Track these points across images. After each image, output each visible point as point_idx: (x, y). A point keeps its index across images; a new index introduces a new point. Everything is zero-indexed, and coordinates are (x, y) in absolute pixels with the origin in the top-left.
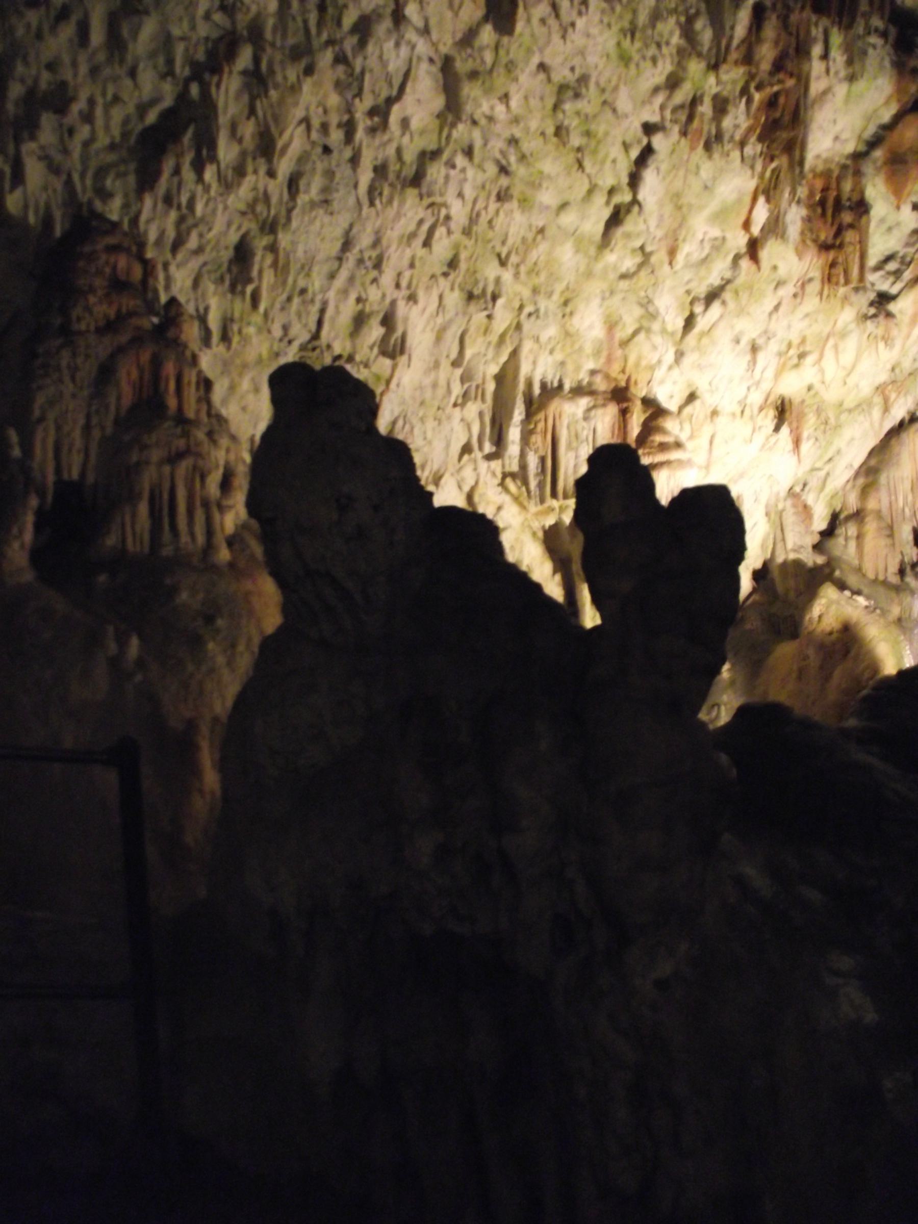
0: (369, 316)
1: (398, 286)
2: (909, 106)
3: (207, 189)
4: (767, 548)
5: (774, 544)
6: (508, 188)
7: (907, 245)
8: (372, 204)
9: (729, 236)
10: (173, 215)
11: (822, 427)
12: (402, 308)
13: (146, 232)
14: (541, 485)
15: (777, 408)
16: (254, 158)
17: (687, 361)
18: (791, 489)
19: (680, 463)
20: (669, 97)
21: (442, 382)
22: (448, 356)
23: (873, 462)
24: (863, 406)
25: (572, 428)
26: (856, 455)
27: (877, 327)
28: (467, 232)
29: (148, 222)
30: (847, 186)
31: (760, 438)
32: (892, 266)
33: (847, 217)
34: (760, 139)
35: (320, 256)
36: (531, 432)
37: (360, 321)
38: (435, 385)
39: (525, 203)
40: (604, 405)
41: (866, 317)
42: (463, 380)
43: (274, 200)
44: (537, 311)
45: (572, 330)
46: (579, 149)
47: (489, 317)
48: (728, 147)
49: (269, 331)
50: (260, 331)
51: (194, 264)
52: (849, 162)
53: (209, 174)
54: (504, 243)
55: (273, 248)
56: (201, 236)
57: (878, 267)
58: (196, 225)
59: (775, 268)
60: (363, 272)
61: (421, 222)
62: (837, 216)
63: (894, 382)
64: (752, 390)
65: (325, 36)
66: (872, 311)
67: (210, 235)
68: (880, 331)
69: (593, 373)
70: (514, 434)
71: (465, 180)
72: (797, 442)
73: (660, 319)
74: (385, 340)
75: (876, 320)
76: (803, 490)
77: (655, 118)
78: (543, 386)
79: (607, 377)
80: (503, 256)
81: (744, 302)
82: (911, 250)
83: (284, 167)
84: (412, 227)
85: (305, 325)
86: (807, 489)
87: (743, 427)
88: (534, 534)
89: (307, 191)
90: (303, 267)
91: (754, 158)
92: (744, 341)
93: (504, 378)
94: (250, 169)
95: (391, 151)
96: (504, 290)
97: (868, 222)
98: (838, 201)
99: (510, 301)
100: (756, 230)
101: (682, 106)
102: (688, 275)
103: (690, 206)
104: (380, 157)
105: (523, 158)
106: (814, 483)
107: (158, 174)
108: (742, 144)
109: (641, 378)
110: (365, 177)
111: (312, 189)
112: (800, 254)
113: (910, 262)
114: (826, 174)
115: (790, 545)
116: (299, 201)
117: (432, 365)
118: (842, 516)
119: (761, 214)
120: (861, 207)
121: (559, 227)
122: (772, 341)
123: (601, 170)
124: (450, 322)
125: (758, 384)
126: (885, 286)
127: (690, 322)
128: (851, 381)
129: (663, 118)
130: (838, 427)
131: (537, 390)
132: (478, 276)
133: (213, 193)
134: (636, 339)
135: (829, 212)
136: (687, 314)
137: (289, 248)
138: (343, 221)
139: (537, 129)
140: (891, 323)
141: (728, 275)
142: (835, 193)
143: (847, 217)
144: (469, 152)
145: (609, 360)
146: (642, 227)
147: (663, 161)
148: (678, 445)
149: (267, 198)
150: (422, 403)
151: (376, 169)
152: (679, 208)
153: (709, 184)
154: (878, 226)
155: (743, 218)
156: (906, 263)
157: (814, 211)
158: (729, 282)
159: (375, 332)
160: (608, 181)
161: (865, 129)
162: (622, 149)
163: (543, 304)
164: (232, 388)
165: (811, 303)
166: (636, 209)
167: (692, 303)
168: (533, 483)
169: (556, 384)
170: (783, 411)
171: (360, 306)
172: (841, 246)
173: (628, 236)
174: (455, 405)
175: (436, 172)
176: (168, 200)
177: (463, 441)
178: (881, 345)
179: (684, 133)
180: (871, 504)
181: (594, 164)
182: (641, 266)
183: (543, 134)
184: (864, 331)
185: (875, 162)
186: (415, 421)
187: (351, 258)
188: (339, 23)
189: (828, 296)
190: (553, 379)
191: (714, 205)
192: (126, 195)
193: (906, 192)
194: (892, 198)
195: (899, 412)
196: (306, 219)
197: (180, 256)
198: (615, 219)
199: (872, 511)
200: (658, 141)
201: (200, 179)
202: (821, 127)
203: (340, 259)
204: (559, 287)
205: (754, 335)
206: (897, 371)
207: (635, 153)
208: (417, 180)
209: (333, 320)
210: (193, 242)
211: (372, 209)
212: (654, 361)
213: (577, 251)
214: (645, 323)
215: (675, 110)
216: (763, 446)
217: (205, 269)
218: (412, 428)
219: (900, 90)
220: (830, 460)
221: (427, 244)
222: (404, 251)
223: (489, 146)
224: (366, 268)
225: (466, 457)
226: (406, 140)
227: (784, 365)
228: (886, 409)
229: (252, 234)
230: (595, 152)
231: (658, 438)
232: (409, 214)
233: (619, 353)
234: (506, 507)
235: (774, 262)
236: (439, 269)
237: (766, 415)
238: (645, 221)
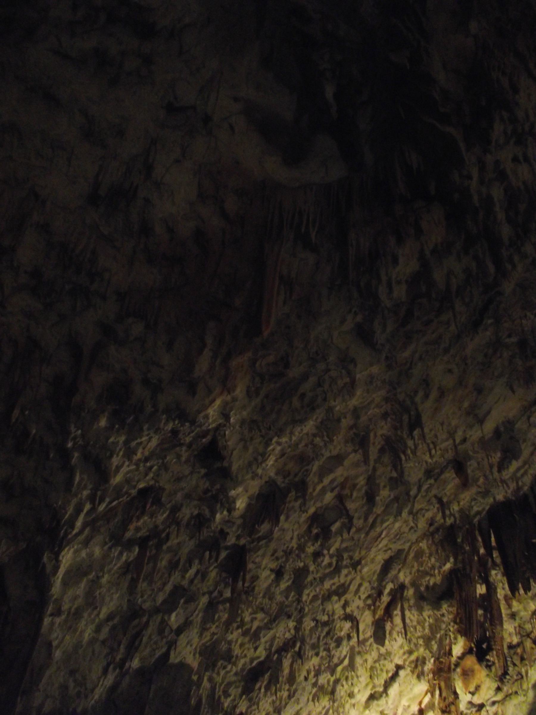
2: (468, 651)
7: (467, 709)
16: (285, 684)
20: (408, 657)
65: (324, 642)
82: (469, 712)
101: (413, 661)
166: (384, 695)
188: (332, 639)
191: (411, 696)
198: (372, 697)
207: (390, 674)
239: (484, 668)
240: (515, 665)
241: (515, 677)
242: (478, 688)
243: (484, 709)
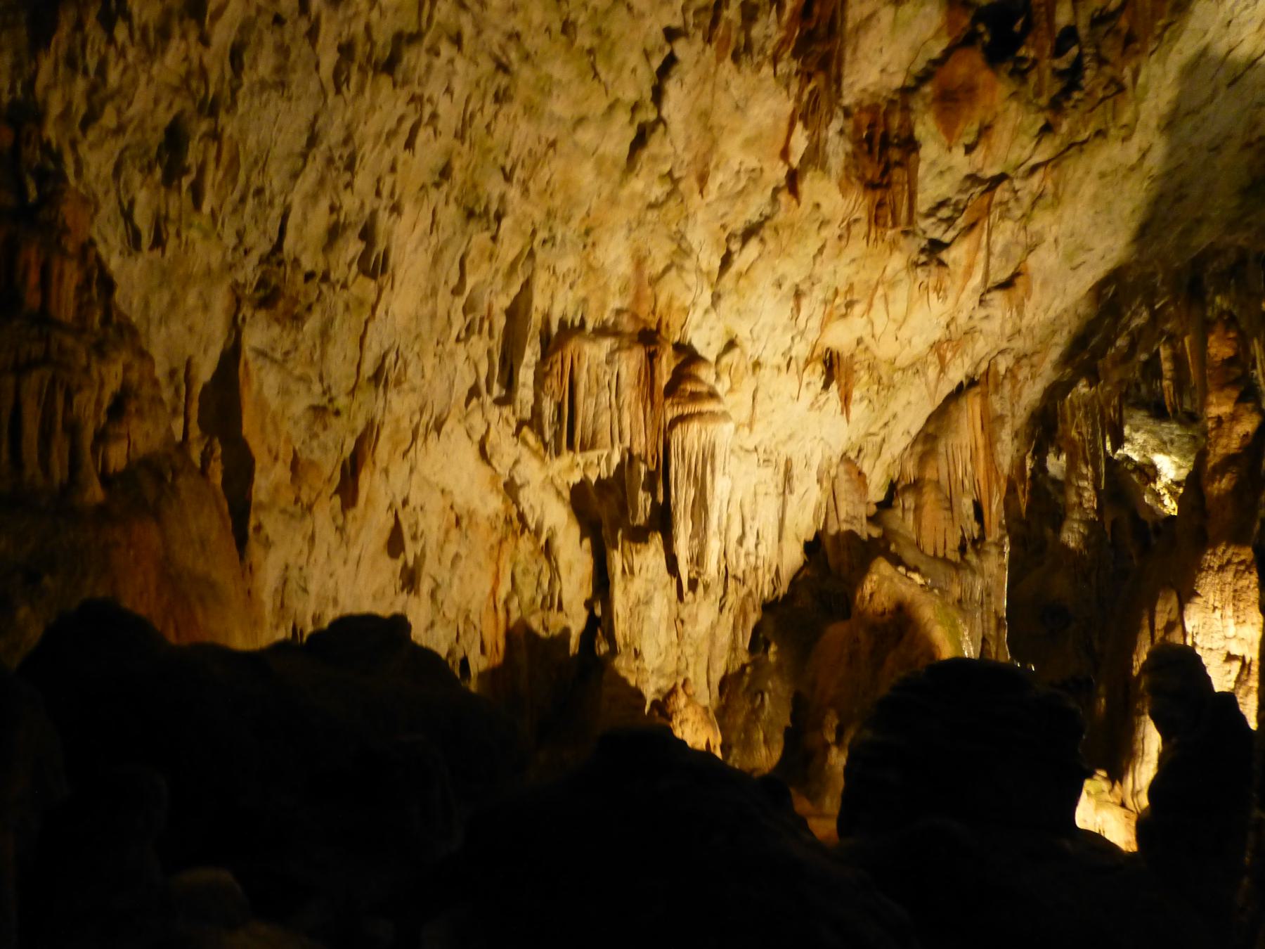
0: (345, 227)
1: (378, 194)
3: (122, 54)
4: (819, 518)
5: (827, 514)
6: (507, 89)
7: (960, 191)
8: (338, 91)
9: (766, 166)
10: (81, 85)
11: (875, 387)
12: (384, 219)
13: (45, 102)
14: (557, 435)
15: (825, 362)
16: (181, 19)
17: (724, 304)
18: (845, 454)
19: (712, 414)
21: (441, 311)
22: (446, 282)
23: (931, 429)
24: (916, 367)
25: (592, 371)
26: (914, 421)
27: (928, 276)
28: (460, 135)
29: (47, 88)
30: (895, 121)
31: (807, 396)
32: (945, 213)
33: (895, 155)
34: (795, 55)
35: (277, 151)
36: (546, 375)
37: (334, 233)
38: (433, 316)
39: (531, 110)
40: (630, 348)
41: (916, 265)
42: (465, 311)
43: (214, 76)
44: (553, 238)
45: (594, 263)
46: (591, 52)
47: (494, 239)
48: (757, 59)
49: (220, 237)
50: (206, 236)
51: (114, 146)
52: (896, 97)
53: (121, 33)
54: (507, 153)
55: (215, 135)
56: (119, 112)
57: (931, 213)
58: (111, 97)
59: (818, 206)
60: (334, 174)
61: (401, 119)
62: (883, 155)
63: (949, 340)
64: (797, 339)
66: (923, 258)
67: (132, 112)
68: (932, 281)
69: (619, 312)
70: (526, 375)
71: (454, 72)
72: (846, 400)
73: (694, 257)
74: (364, 257)
75: (927, 268)
76: (858, 456)
77: (677, 23)
78: (562, 323)
79: (635, 317)
80: (508, 169)
81: (784, 243)
82: (965, 197)
83: (223, 34)
84: (392, 124)
85: (265, 232)
86: (862, 455)
87: (788, 384)
88: (559, 493)
89: (254, 66)
90: (256, 162)
91: (789, 76)
92: (787, 286)
93: (517, 313)
94: (177, 32)
95: (358, 28)
96: (509, 209)
97: (918, 161)
98: (885, 136)
99: (518, 223)
100: (795, 161)
102: (723, 208)
103: (722, 128)
104: (344, 34)
105: (526, 57)
106: (869, 449)
107: (53, 27)
108: (775, 60)
109: (675, 320)
110: (329, 59)
111: (264, 66)
112: (844, 192)
113: (963, 210)
114: (873, 109)
115: (842, 516)
116: (246, 81)
117: (429, 292)
118: (899, 487)
119: (800, 142)
120: (911, 145)
121: (576, 144)
122: (817, 287)
123: (618, 77)
124: (447, 242)
125: (802, 333)
126: (937, 234)
127: (726, 261)
128: (905, 333)
129: (685, 22)
130: (891, 386)
131: (554, 328)
132: (480, 190)
133: (130, 58)
134: (667, 277)
135: (877, 149)
136: (723, 252)
137: (236, 136)
138: (305, 111)
139: (541, 25)
140: (943, 270)
141: (767, 211)
142: (881, 130)
143: (895, 155)
144: (457, 40)
145: (638, 298)
146: (668, 149)
147: (687, 73)
148: (712, 395)
149: (203, 73)
150: (418, 336)
151: (341, 49)
152: (709, 129)
153: (741, 104)
154: (928, 170)
155: (781, 146)
156: (959, 210)
157: (860, 147)
158: (767, 218)
159: (352, 247)
160: (630, 95)
161: (912, 62)
162: (643, 58)
163: (559, 232)
164: (173, 303)
165: (857, 247)
166: (661, 128)
167: (728, 240)
168: (548, 435)
169: (577, 323)
170: (832, 367)
171: (334, 217)
172: (888, 185)
173: (654, 159)
174: (458, 340)
175: (414, 58)
176: (72, 62)
177: (470, 382)
178: (933, 296)
179: (708, 40)
180: (930, 474)
181: (609, 71)
182: (669, 195)
183: (548, 30)
184: (915, 280)
185: (924, 97)
186: (410, 356)
187: (320, 153)
189: (876, 239)
190: (574, 317)
191: (748, 130)
192: (16, 53)
193: (958, 131)
194: (943, 138)
195: (957, 374)
196: (256, 102)
197: (92, 135)
198: (640, 140)
199: (930, 481)
200: (680, 48)
201: (111, 40)
202: (866, 57)
203: (305, 156)
204: (579, 214)
205: (797, 280)
206: (952, 327)
207: (657, 62)
208: (390, 66)
209: (300, 229)
210: (109, 119)
211: (340, 98)
212: (688, 303)
213: (599, 173)
214: (677, 260)
215: (696, 13)
216: (812, 404)
217: (127, 154)
218: (406, 364)
219: (951, 23)
220: (886, 424)
221: (409, 145)
222: (382, 152)
223: (484, 37)
224: (337, 169)
225: (474, 402)
226: (375, 14)
227: (831, 314)
228: (943, 370)
229: (187, 115)
230: (609, 56)
231: (690, 387)
232: (386, 108)
233: (649, 291)
234: (523, 460)
235: (817, 199)
236: (428, 179)
237: (814, 371)
238: (672, 142)
239: (1004, 75)
240: (1101, 61)
241: (1100, 94)
242: (985, 131)
243: (1005, 184)
